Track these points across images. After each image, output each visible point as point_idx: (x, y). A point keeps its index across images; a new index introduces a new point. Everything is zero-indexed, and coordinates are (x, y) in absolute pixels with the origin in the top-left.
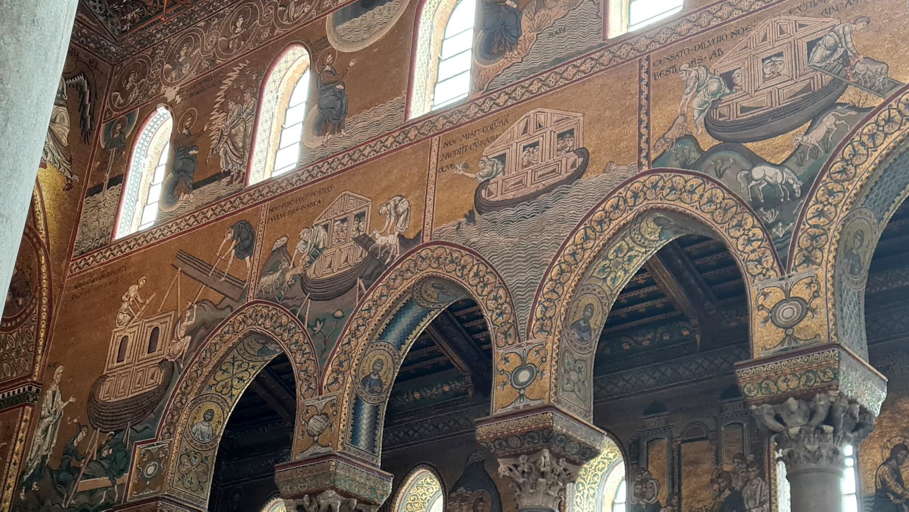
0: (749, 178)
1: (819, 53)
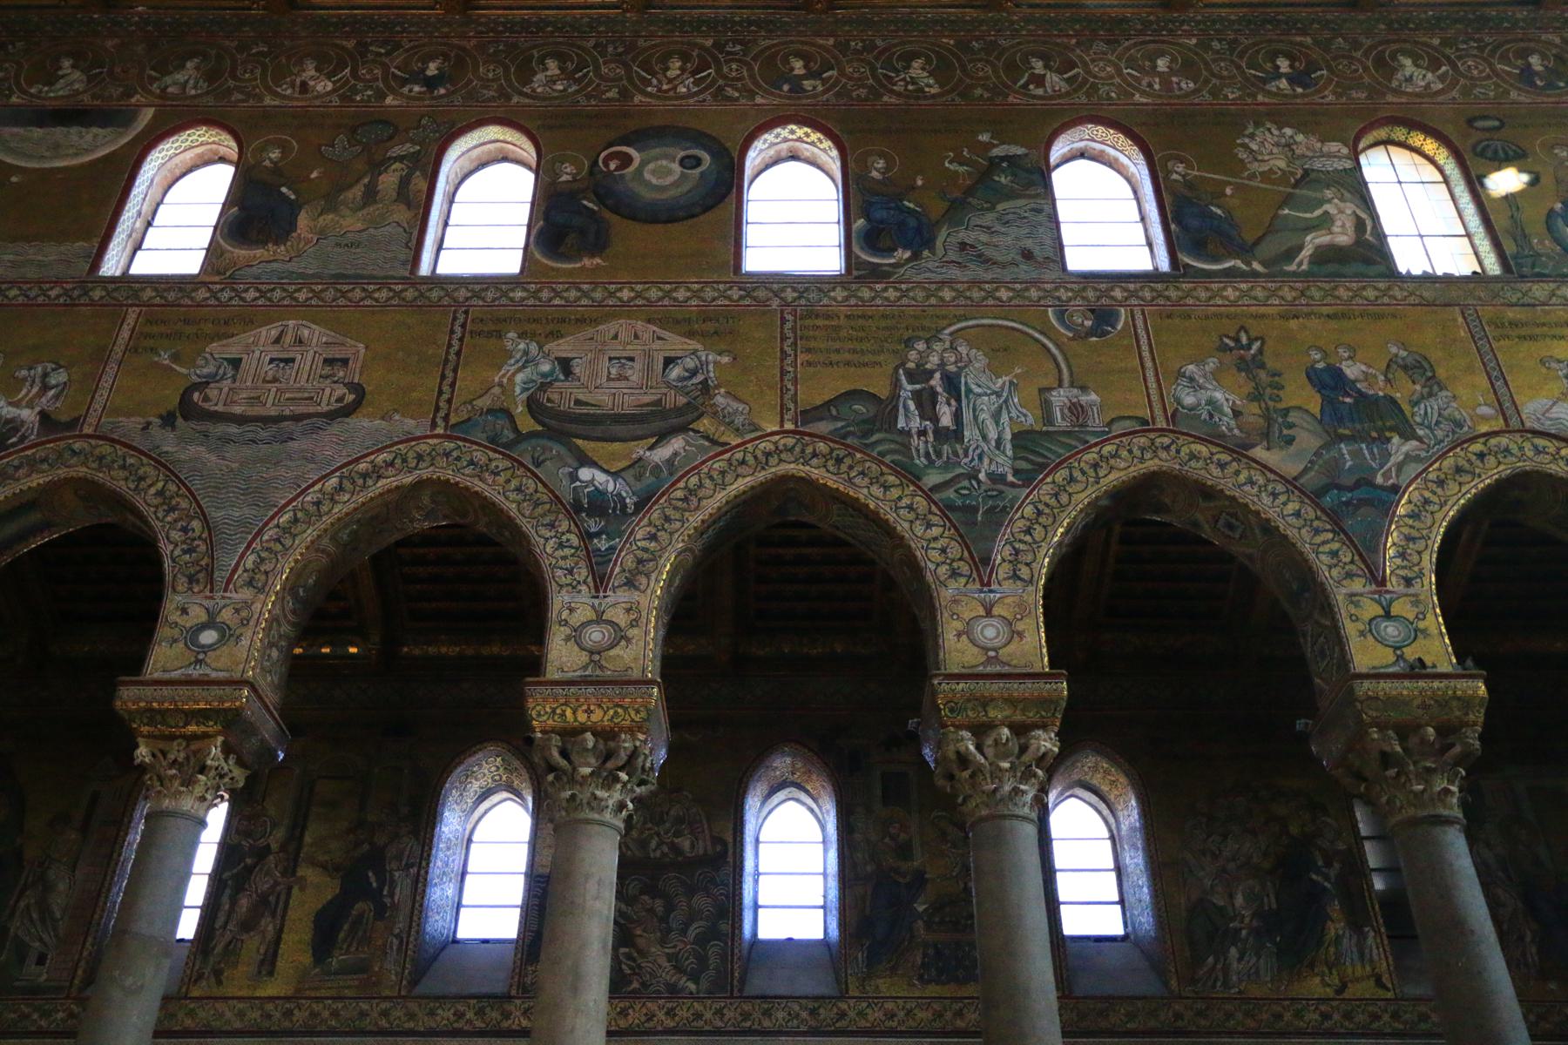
0: (574, 477)
1: (675, 372)
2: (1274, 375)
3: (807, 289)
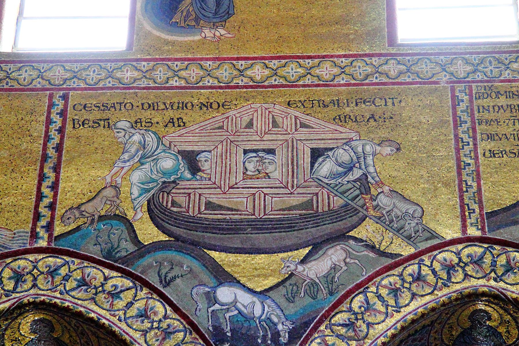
3: (482, 61)
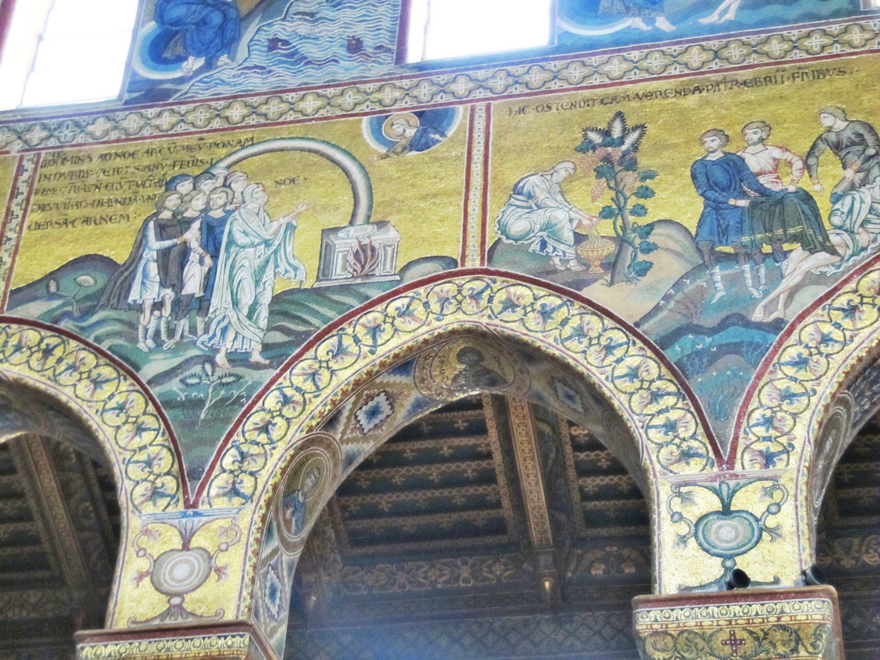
2: (644, 179)
3: (60, 126)
